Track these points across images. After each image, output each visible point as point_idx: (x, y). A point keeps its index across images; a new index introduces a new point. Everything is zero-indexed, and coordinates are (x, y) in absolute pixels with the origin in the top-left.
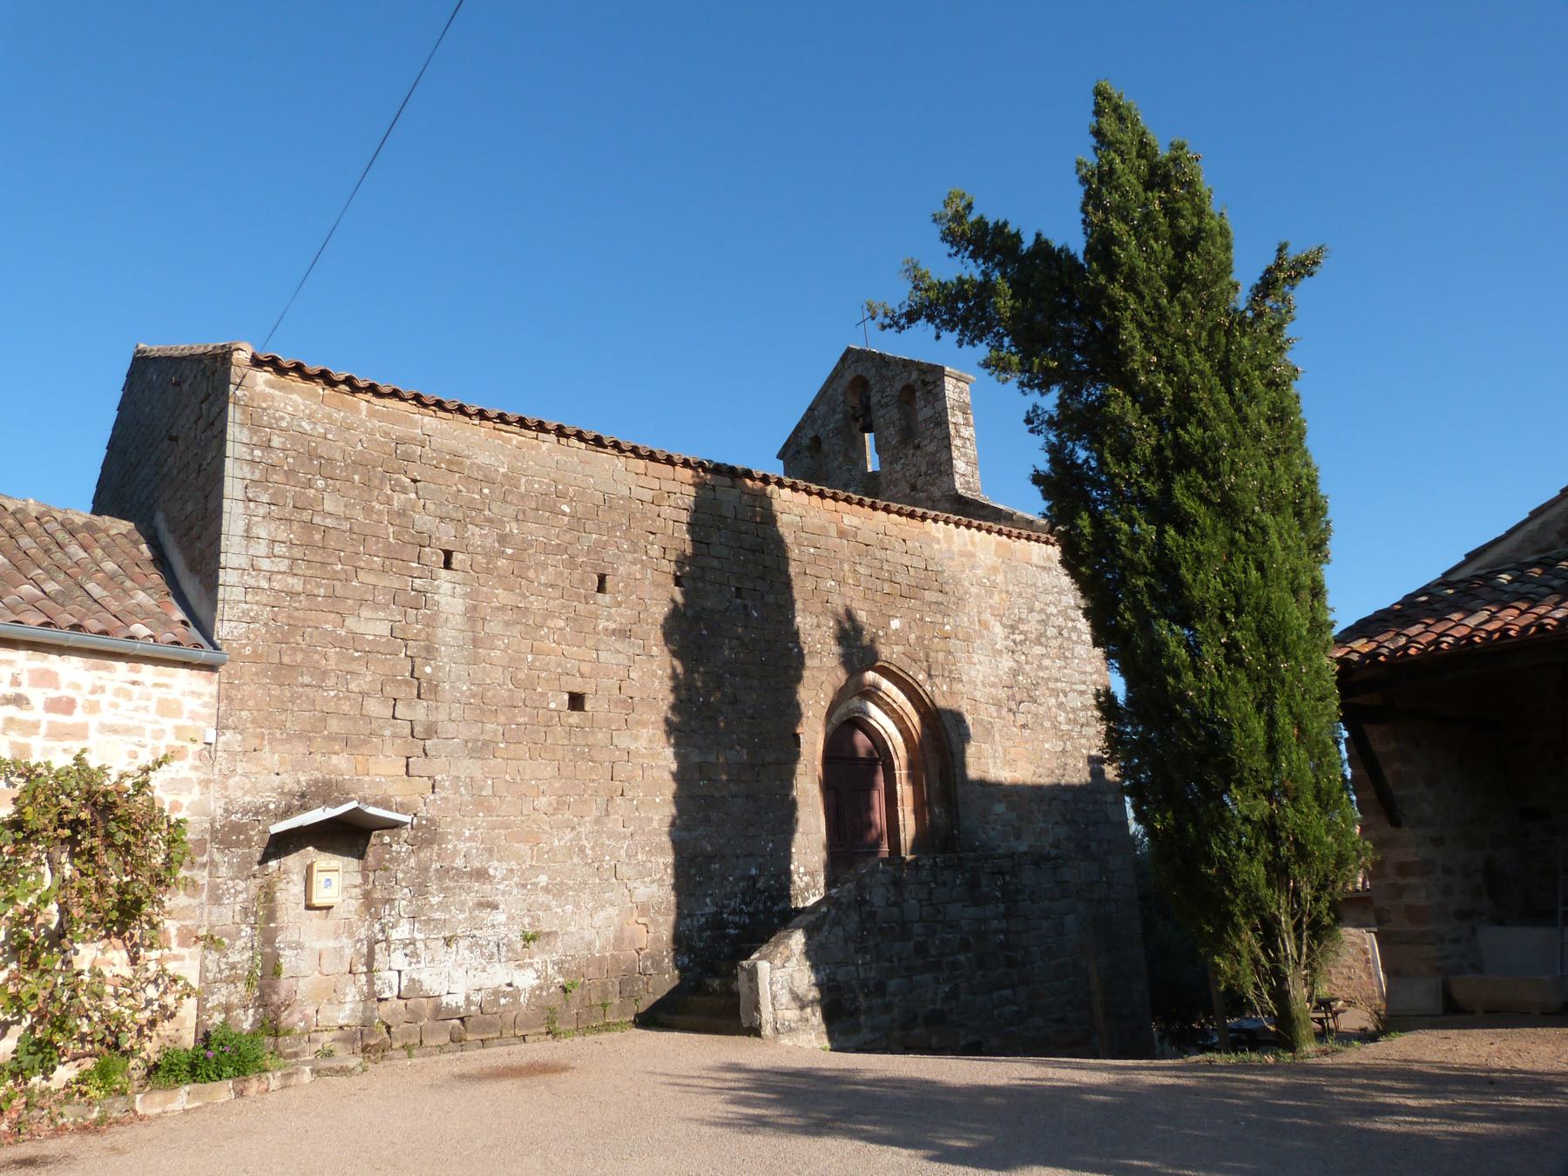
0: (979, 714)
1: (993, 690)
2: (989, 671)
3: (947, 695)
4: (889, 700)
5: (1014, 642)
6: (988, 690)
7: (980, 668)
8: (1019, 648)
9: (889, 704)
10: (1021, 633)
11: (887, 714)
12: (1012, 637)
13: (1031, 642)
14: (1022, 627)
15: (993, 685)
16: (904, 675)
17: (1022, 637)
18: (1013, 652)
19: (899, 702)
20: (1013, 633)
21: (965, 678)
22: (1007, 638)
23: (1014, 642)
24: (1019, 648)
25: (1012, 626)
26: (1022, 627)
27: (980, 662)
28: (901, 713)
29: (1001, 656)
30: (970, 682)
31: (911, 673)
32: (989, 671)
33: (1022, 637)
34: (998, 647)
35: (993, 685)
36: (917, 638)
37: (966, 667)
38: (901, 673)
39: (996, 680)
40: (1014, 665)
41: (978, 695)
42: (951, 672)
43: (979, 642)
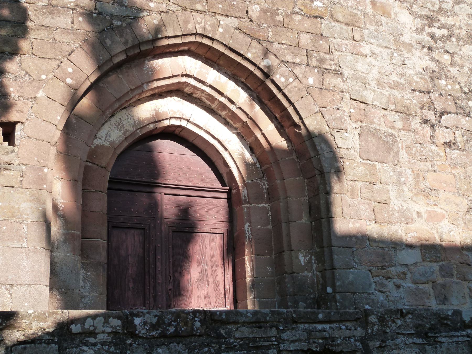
0: (372, 122)
1: (396, 93)
2: (389, 68)
3: (315, 92)
4: (222, 99)
5: (433, 37)
6: (387, 91)
7: (374, 62)
8: (440, 44)
9: (224, 107)
10: (443, 27)
11: (226, 123)
12: (428, 30)
13: (459, 39)
14: (443, 20)
15: (396, 86)
16: (238, 59)
17: (445, 32)
18: (430, 48)
19: (209, 81)
20: (430, 26)
21: (347, 72)
22: (419, 30)
23: (433, 37)
24: (440, 44)
25: (428, 17)
26: (443, 20)
27: (374, 55)
28: (244, 118)
29: (410, 51)
30: (355, 78)
31: (249, 55)
32: (389, 68)
33: (445, 32)
34: (406, 38)
35: (396, 86)
36: (264, 11)
37: (350, 57)
38: (233, 56)
39: (402, 81)
40: (433, 66)
41: (369, 96)
42: (322, 61)
43: (372, 28)
